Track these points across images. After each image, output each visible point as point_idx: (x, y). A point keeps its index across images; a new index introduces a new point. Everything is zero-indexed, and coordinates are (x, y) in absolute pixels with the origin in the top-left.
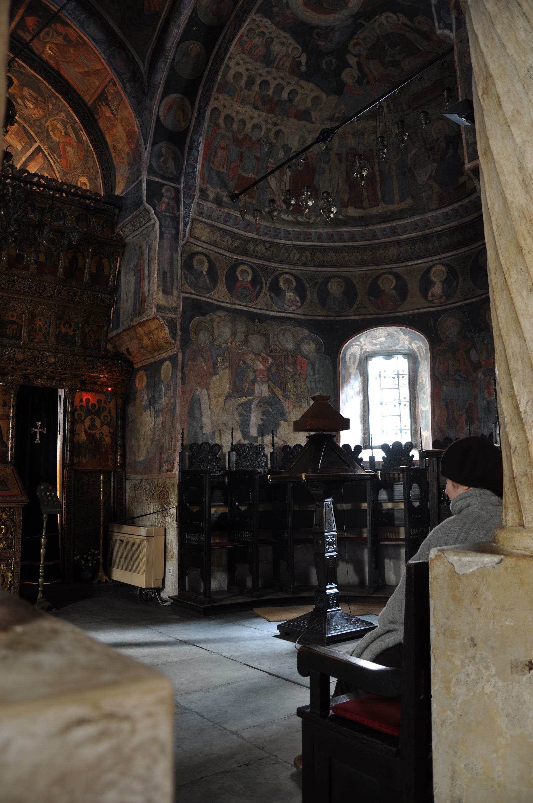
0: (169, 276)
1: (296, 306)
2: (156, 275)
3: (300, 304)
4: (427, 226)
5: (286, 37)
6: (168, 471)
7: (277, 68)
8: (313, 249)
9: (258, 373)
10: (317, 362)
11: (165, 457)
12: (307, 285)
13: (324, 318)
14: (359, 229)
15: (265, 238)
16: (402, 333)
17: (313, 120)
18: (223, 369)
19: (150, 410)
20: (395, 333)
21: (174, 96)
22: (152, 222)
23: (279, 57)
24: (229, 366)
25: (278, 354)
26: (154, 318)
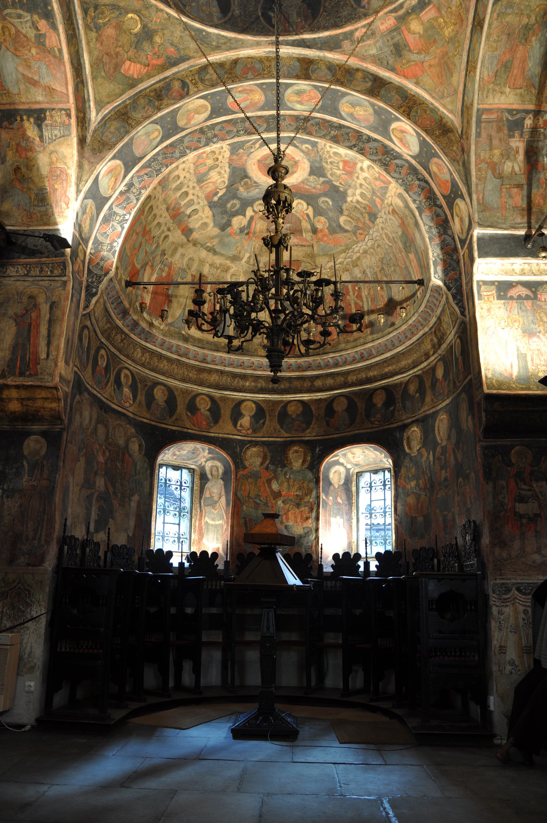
0: (70, 344)
2: (63, 340)
3: (132, 403)
5: (225, 171)
6: (29, 565)
7: (201, 188)
8: (153, 353)
10: (139, 463)
12: (139, 385)
13: (147, 421)
14: (196, 349)
15: (126, 330)
16: (207, 451)
17: (190, 239)
20: (201, 450)
21: (118, 162)
22: (64, 279)
23: (209, 181)
26: (56, 388)
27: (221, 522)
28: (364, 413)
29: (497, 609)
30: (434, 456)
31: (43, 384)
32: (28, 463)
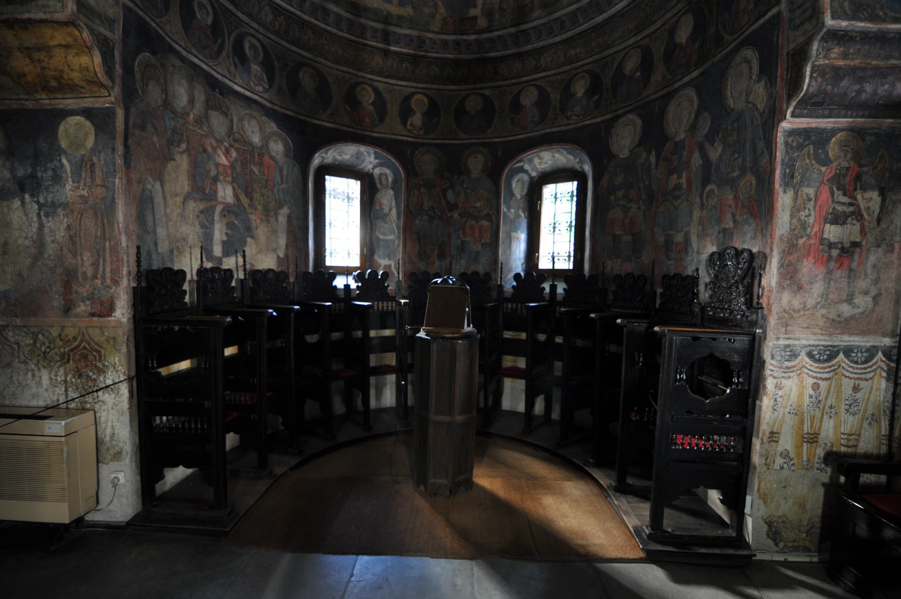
1: (264, 88)
3: (267, 87)
4: (421, 47)
6: (93, 315)
8: (290, 17)
9: (221, 170)
10: (285, 168)
11: (84, 290)
12: (276, 63)
13: (293, 114)
16: (373, 156)
18: (180, 153)
19: (23, 203)
20: (366, 154)
24: (187, 150)
25: (243, 147)
27: (392, 237)
28: (558, 106)
29: (775, 381)
30: (658, 157)
31: (48, 16)
32: (69, 161)
